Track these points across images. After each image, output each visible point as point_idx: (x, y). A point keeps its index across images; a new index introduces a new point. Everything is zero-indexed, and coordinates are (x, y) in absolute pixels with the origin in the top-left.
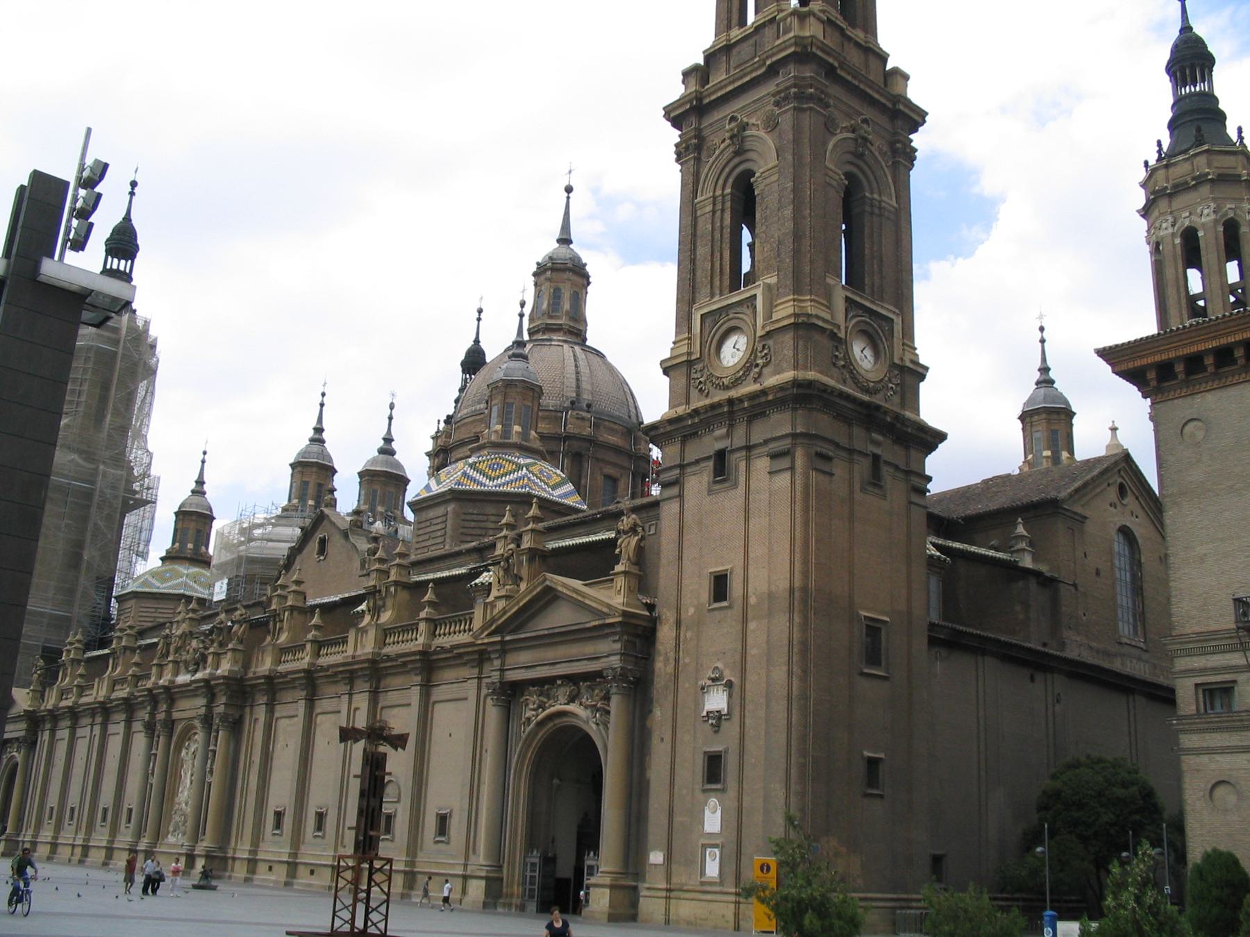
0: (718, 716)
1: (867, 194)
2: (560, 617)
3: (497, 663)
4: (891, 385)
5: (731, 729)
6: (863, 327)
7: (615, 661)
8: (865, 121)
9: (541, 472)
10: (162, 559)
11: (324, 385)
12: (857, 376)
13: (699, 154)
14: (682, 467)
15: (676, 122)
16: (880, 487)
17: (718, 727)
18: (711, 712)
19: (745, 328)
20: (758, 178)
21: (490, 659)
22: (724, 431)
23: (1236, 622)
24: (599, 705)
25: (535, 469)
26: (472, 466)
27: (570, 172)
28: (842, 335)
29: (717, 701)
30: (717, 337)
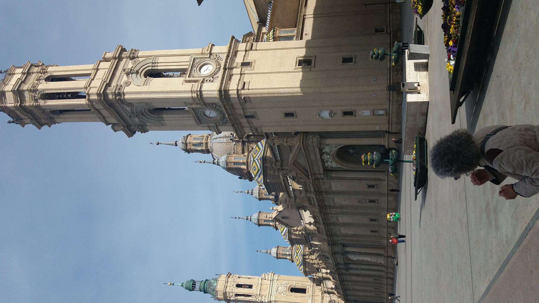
0: (330, 114)
2: (302, 161)
3: (318, 176)
8: (124, 70)
9: (255, 154)
11: (232, 218)
13: (144, 125)
14: (251, 127)
16: (252, 62)
19: (203, 111)
20: (150, 107)
21: (317, 177)
24: (330, 147)
25: (254, 156)
29: (326, 114)
30: (207, 119)
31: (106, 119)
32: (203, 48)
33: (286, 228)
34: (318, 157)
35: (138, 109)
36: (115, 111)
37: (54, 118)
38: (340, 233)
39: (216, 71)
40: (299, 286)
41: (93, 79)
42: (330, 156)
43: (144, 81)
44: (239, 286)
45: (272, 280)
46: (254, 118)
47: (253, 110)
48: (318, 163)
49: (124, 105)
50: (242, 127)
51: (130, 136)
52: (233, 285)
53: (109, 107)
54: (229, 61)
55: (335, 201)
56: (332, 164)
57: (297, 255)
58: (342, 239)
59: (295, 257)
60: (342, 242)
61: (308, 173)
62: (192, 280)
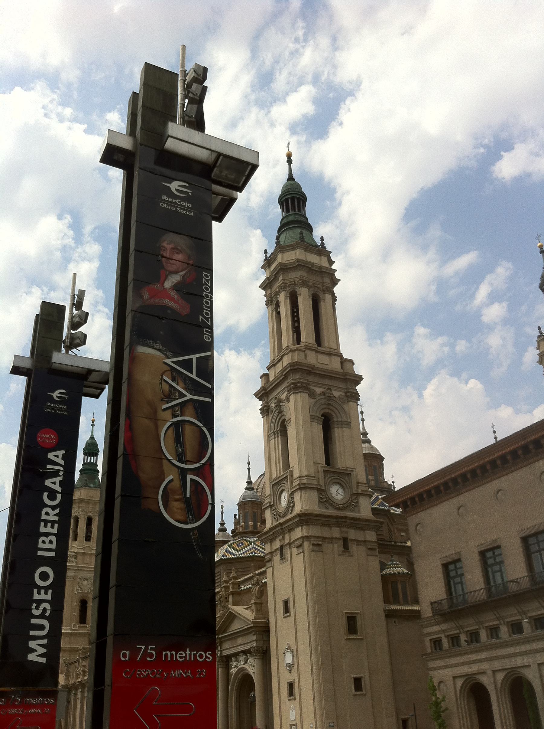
1: (335, 420)
2: (236, 626)
5: (295, 670)
6: (336, 480)
7: (254, 644)
8: (330, 389)
13: (268, 413)
15: (260, 399)
16: (349, 552)
17: (291, 670)
18: (288, 664)
22: (281, 537)
23: (433, 613)
26: (230, 546)
28: (323, 488)
29: (289, 659)
30: (278, 494)
31: (273, 367)
34: (241, 648)
37: (271, 305)
39: (335, 505)
41: (317, 352)
42: (244, 664)
43: (317, 415)
46: (281, 557)
49: (286, 393)
51: (256, 395)
52: (90, 512)
54: (348, 521)
61: (222, 633)
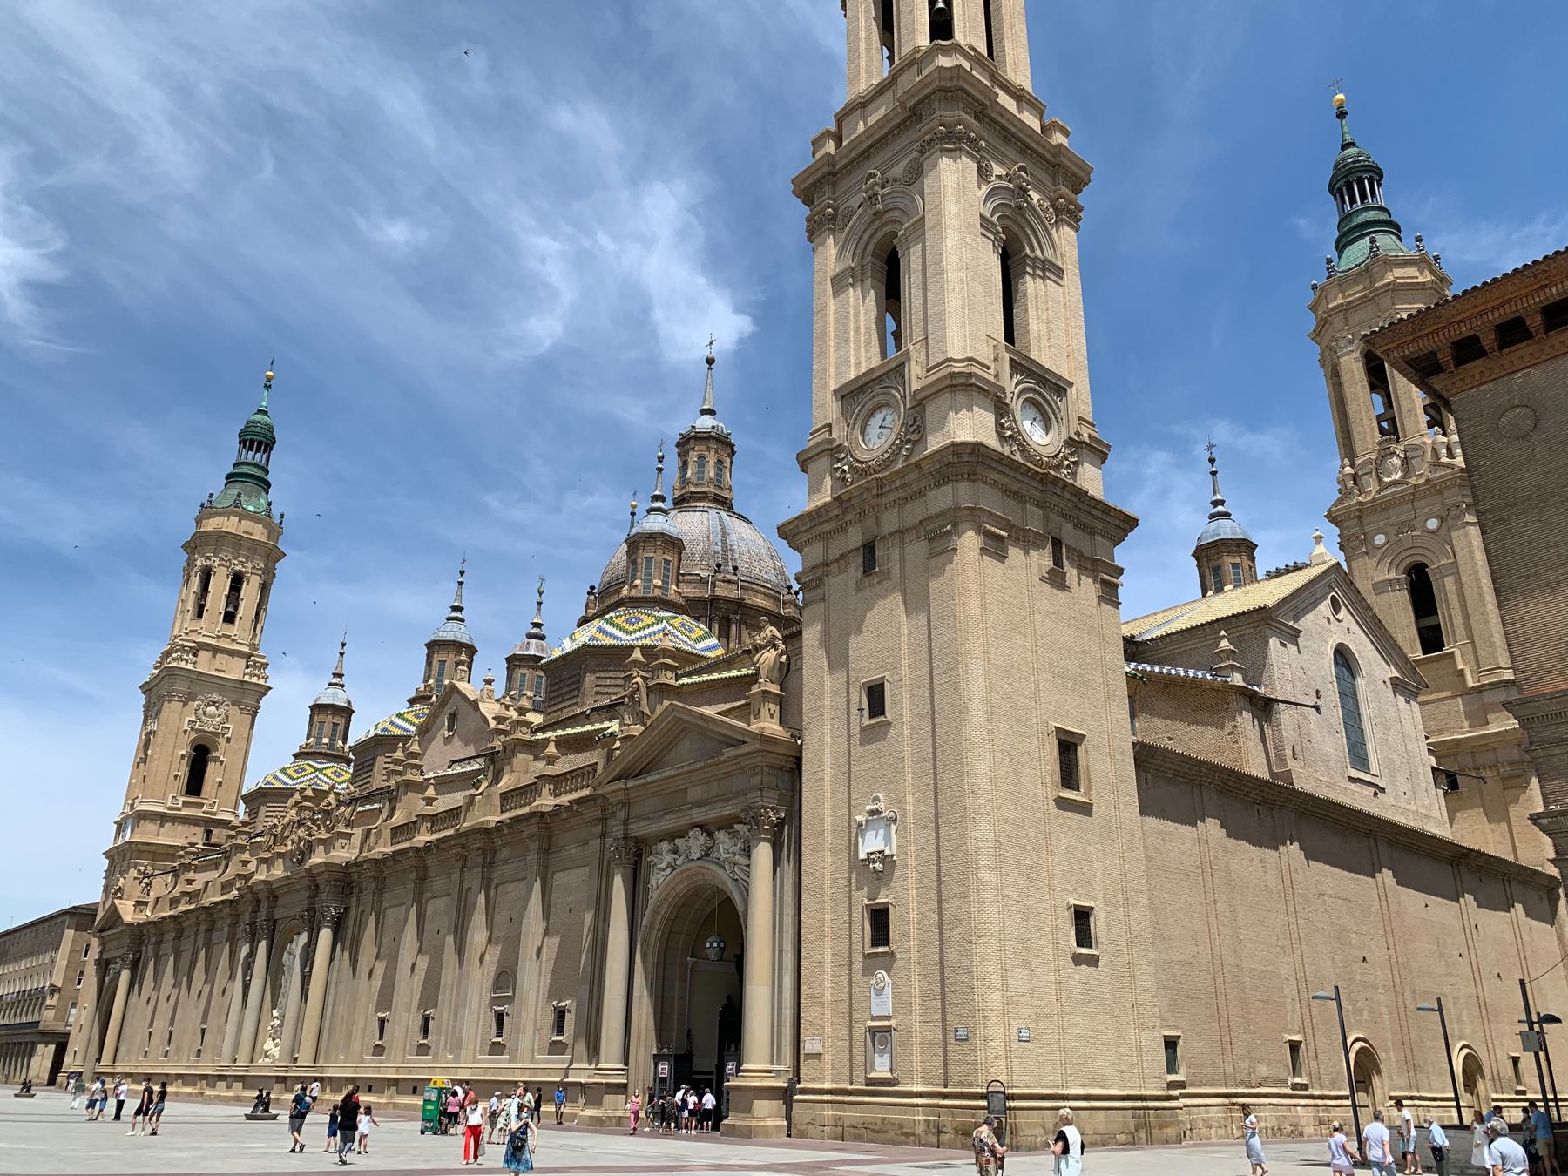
4: (1066, 463)
6: (1032, 395)
9: (682, 625)
10: (296, 756)
12: (1028, 448)
14: (826, 564)
18: (872, 853)
25: (676, 622)
27: (711, 343)
32: (1093, 426)
33: (414, 729)
34: (699, 815)
35: (898, 200)
36: (890, 132)
38: (385, 904)
40: (212, 773)
44: (237, 580)
45: (245, 687)
47: (896, 571)
48: (673, 816)
50: (825, 537)
53: (908, 106)
55: (510, 887)
56: (664, 870)
57: (316, 770)
58: (363, 911)
59: (310, 762)
60: (353, 910)
62: (274, 443)
